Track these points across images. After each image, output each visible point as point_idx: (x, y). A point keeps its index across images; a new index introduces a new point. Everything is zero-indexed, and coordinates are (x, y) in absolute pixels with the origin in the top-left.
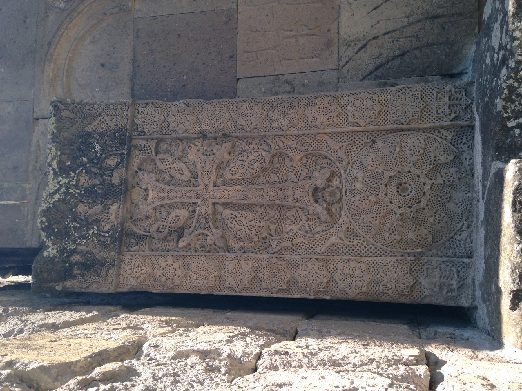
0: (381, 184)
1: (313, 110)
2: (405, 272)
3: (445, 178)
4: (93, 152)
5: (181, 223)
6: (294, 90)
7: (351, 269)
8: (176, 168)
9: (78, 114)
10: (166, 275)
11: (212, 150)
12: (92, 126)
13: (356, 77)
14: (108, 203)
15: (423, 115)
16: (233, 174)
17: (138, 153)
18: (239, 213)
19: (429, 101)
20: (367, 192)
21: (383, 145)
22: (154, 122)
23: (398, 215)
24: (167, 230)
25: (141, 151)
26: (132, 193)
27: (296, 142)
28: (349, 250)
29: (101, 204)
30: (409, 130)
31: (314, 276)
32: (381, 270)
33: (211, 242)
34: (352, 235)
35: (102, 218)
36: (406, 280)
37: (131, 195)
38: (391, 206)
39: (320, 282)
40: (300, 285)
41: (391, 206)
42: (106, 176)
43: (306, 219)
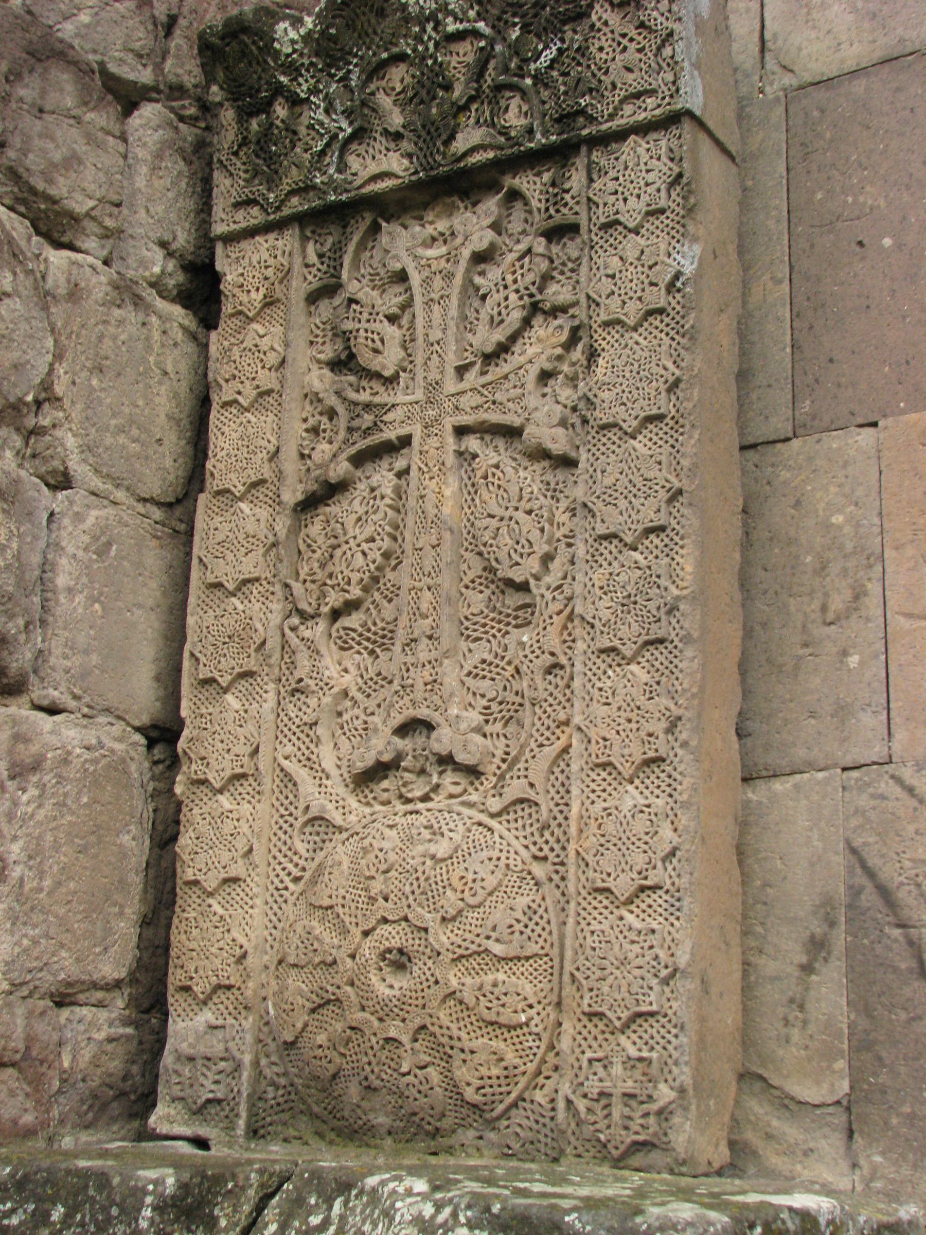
1: (634, 691)
2: (220, 973)
3: (416, 1076)
4: (536, 48)
5: (365, 358)
6: (831, 623)
7: (230, 838)
13: (861, 826)
15: (595, 1020)
16: (486, 477)
17: (546, 177)
19: (634, 1037)
22: (625, 200)
23: (334, 951)
25: (553, 184)
26: (448, 200)
27: (558, 651)
31: (219, 745)
34: (317, 839)
39: (208, 764)
41: (357, 932)
42: (477, 110)
43: (369, 711)
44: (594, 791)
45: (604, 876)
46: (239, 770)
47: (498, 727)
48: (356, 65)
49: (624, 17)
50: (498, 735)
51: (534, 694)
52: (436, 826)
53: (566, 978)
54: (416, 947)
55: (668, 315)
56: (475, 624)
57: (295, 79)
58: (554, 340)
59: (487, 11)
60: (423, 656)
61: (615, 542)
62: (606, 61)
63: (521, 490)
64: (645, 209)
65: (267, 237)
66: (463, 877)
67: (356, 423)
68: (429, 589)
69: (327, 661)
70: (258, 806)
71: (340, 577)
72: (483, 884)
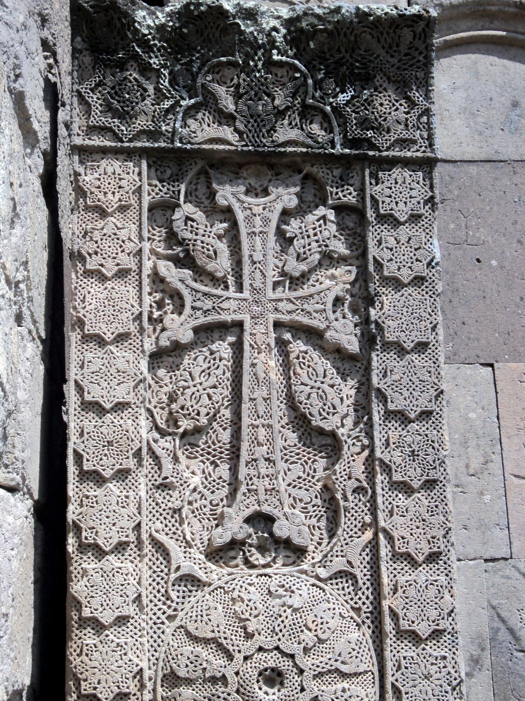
0: (279, 640)
4: (335, 89)
8: (308, 247)
9: (406, 58)
10: (104, 241)
11: (344, 317)
12: (385, 85)
14: (237, 124)
17: (337, 172)
18: (224, 373)
20: (266, 614)
21: (353, 641)
22: (397, 203)
23: (222, 670)
24: (188, 235)
25: (341, 178)
28: (158, 583)
29: (236, 111)
30: (382, 687)
32: (122, 641)
33: (167, 321)
34: (185, 589)
35: (210, 113)
36: (106, 686)
37: (256, 163)
38: (239, 657)
39: (97, 532)
40: (92, 493)
42: (290, 116)
43: (214, 503)
44: (395, 569)
45: (410, 623)
46: (124, 539)
47: (314, 521)
48: (197, 58)
49: (397, 89)
50: (314, 527)
51: (347, 504)
52: (287, 586)
53: (389, 687)
54: (286, 667)
55: (427, 281)
56: (291, 452)
57: (147, 53)
58: (344, 279)
59: (301, 55)
60: (263, 471)
61: (399, 416)
62: (385, 113)
63: (325, 371)
64: (410, 212)
65: (117, 156)
66: (313, 621)
67: (198, 304)
68: (263, 426)
69: (182, 467)
70: (140, 565)
71: (191, 409)
72: (328, 625)
